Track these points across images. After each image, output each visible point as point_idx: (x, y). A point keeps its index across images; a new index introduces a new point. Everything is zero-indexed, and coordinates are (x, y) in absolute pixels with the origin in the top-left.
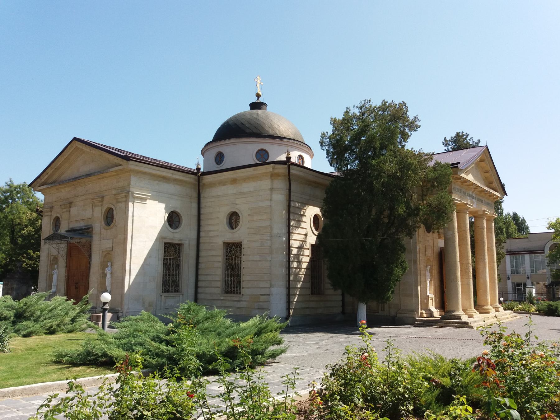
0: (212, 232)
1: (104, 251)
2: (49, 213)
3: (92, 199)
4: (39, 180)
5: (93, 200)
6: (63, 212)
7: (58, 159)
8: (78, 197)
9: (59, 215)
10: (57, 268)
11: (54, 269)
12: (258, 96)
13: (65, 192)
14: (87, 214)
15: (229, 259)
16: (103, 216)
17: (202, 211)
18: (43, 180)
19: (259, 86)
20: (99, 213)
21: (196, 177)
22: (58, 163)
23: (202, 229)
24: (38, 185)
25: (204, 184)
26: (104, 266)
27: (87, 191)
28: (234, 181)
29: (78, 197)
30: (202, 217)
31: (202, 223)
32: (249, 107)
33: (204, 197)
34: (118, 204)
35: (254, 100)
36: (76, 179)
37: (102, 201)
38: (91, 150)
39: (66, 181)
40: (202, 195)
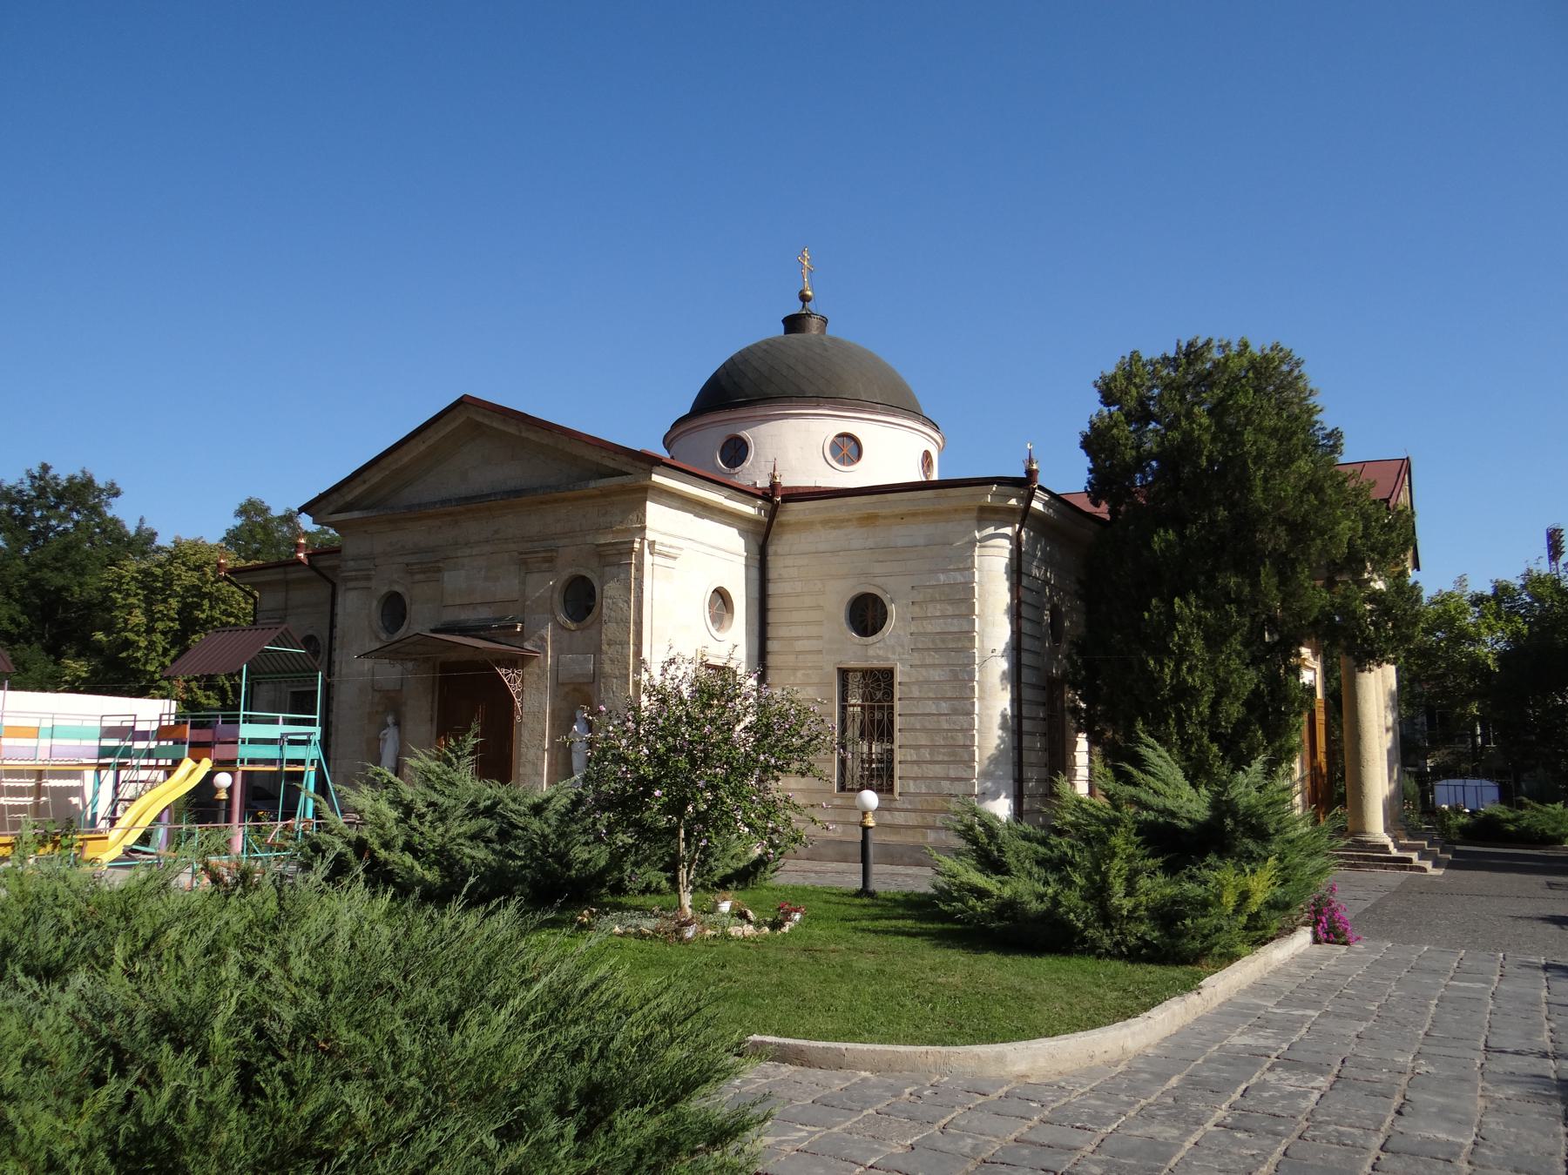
0: (800, 642)
1: (563, 684)
2: (363, 584)
3: (521, 553)
4: (335, 496)
5: (521, 556)
6: (414, 583)
7: (405, 448)
8: (466, 544)
9: (397, 588)
10: (397, 724)
11: (386, 726)
12: (804, 298)
13: (416, 535)
14: (506, 585)
15: (872, 708)
16: (556, 596)
17: (773, 589)
18: (349, 498)
19: (806, 272)
20: (547, 586)
21: (769, 506)
22: (406, 457)
23: (772, 632)
24: (331, 509)
25: (781, 525)
26: (563, 723)
27: (496, 532)
28: (869, 520)
29: (466, 544)
30: (772, 603)
31: (772, 617)
32: (782, 327)
33: (776, 554)
34: (607, 569)
35: (796, 308)
36: (468, 499)
37: (550, 560)
38: (520, 432)
39: (436, 503)
40: (771, 549)
